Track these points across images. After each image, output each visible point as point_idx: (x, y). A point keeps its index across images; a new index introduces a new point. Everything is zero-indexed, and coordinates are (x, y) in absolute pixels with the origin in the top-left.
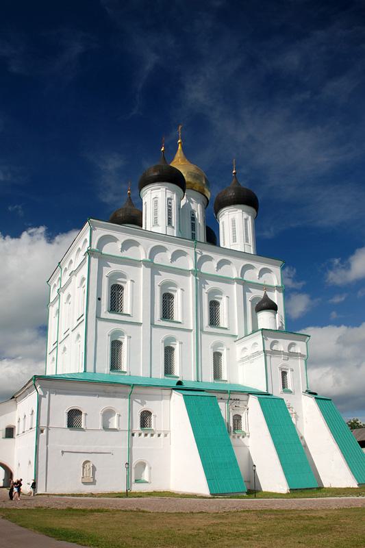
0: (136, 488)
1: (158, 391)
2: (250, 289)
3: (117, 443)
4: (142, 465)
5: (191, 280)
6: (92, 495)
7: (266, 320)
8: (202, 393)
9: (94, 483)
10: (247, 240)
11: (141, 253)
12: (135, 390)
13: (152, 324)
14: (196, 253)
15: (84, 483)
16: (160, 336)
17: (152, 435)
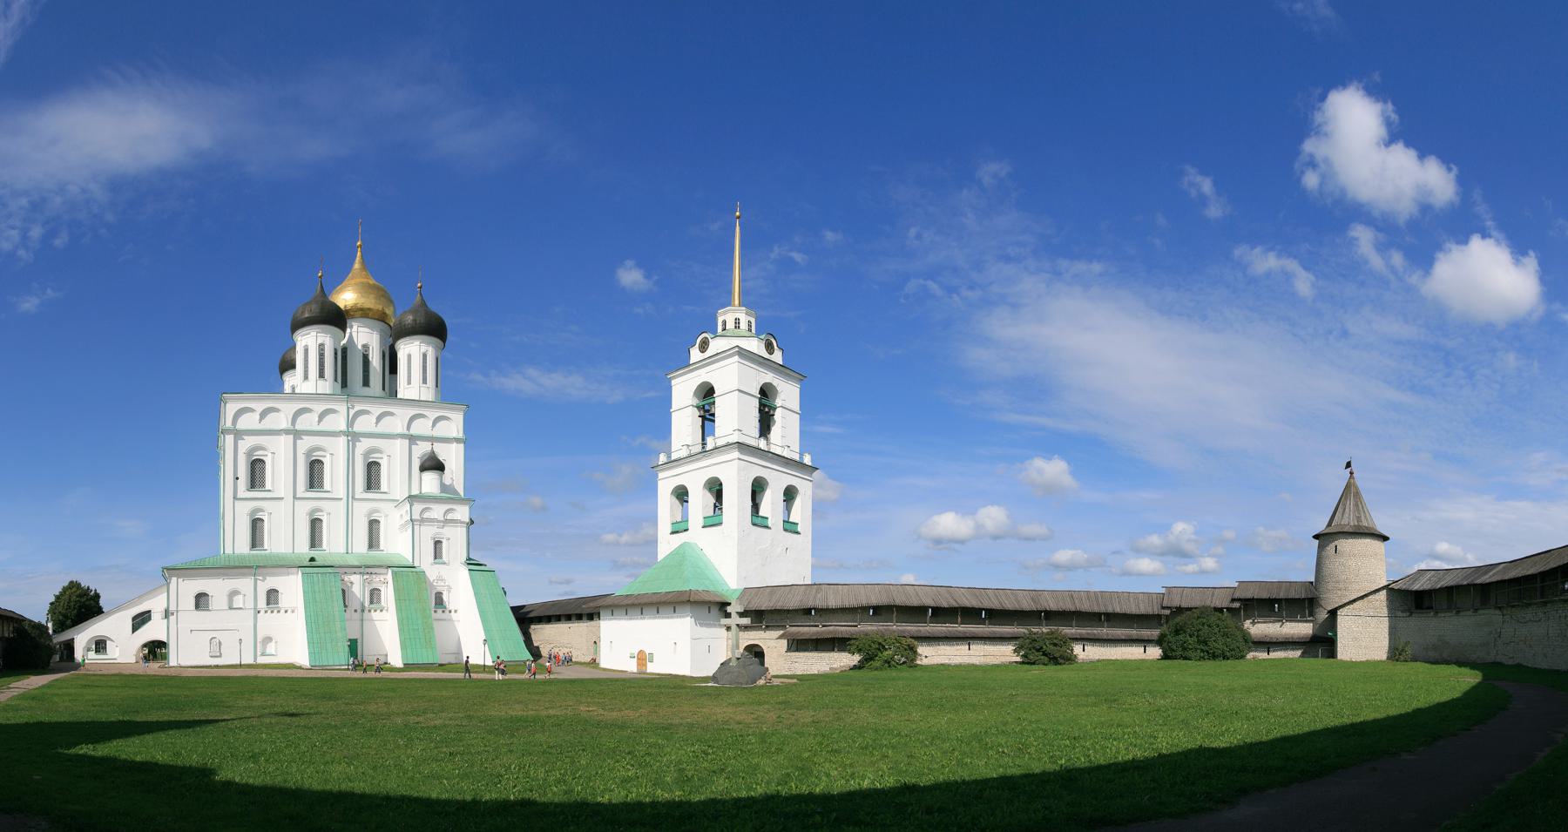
0: (261, 660)
1: (285, 570)
2: (418, 442)
3: (243, 620)
4: (268, 639)
5: (342, 441)
6: (217, 666)
7: (430, 482)
8: (329, 570)
9: (220, 656)
10: (425, 381)
11: (281, 420)
12: (258, 571)
13: (295, 498)
14: (348, 408)
15: (212, 657)
16: (303, 509)
17: (279, 612)
